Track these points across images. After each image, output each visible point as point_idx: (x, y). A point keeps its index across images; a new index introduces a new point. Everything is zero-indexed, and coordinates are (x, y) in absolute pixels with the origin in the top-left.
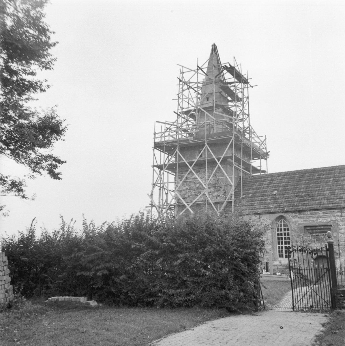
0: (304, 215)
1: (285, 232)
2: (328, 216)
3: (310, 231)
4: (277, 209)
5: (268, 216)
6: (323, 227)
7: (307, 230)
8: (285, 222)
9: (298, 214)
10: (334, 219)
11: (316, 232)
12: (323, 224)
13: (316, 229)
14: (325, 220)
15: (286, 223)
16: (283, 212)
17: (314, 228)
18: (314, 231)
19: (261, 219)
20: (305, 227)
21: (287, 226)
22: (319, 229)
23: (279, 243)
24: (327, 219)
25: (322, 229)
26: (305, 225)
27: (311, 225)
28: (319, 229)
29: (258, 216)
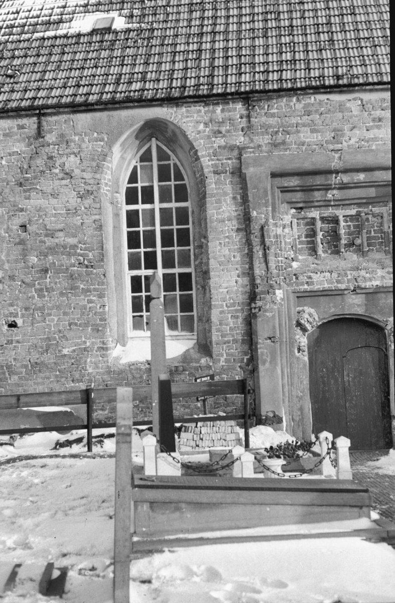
0: (273, 115)
1: (165, 205)
3: (299, 196)
4: (136, 86)
5: (83, 119)
6: (362, 176)
7: (285, 190)
8: (168, 158)
9: (239, 107)
11: (327, 204)
13: (327, 188)
14: (375, 139)
15: (173, 160)
16: (169, 100)
17: (319, 180)
18: (318, 195)
19: (50, 138)
20: (274, 175)
21: (179, 176)
22: (343, 187)
23: (134, 263)
25: (358, 186)
26: (275, 165)
27: (307, 166)
29: (30, 123)
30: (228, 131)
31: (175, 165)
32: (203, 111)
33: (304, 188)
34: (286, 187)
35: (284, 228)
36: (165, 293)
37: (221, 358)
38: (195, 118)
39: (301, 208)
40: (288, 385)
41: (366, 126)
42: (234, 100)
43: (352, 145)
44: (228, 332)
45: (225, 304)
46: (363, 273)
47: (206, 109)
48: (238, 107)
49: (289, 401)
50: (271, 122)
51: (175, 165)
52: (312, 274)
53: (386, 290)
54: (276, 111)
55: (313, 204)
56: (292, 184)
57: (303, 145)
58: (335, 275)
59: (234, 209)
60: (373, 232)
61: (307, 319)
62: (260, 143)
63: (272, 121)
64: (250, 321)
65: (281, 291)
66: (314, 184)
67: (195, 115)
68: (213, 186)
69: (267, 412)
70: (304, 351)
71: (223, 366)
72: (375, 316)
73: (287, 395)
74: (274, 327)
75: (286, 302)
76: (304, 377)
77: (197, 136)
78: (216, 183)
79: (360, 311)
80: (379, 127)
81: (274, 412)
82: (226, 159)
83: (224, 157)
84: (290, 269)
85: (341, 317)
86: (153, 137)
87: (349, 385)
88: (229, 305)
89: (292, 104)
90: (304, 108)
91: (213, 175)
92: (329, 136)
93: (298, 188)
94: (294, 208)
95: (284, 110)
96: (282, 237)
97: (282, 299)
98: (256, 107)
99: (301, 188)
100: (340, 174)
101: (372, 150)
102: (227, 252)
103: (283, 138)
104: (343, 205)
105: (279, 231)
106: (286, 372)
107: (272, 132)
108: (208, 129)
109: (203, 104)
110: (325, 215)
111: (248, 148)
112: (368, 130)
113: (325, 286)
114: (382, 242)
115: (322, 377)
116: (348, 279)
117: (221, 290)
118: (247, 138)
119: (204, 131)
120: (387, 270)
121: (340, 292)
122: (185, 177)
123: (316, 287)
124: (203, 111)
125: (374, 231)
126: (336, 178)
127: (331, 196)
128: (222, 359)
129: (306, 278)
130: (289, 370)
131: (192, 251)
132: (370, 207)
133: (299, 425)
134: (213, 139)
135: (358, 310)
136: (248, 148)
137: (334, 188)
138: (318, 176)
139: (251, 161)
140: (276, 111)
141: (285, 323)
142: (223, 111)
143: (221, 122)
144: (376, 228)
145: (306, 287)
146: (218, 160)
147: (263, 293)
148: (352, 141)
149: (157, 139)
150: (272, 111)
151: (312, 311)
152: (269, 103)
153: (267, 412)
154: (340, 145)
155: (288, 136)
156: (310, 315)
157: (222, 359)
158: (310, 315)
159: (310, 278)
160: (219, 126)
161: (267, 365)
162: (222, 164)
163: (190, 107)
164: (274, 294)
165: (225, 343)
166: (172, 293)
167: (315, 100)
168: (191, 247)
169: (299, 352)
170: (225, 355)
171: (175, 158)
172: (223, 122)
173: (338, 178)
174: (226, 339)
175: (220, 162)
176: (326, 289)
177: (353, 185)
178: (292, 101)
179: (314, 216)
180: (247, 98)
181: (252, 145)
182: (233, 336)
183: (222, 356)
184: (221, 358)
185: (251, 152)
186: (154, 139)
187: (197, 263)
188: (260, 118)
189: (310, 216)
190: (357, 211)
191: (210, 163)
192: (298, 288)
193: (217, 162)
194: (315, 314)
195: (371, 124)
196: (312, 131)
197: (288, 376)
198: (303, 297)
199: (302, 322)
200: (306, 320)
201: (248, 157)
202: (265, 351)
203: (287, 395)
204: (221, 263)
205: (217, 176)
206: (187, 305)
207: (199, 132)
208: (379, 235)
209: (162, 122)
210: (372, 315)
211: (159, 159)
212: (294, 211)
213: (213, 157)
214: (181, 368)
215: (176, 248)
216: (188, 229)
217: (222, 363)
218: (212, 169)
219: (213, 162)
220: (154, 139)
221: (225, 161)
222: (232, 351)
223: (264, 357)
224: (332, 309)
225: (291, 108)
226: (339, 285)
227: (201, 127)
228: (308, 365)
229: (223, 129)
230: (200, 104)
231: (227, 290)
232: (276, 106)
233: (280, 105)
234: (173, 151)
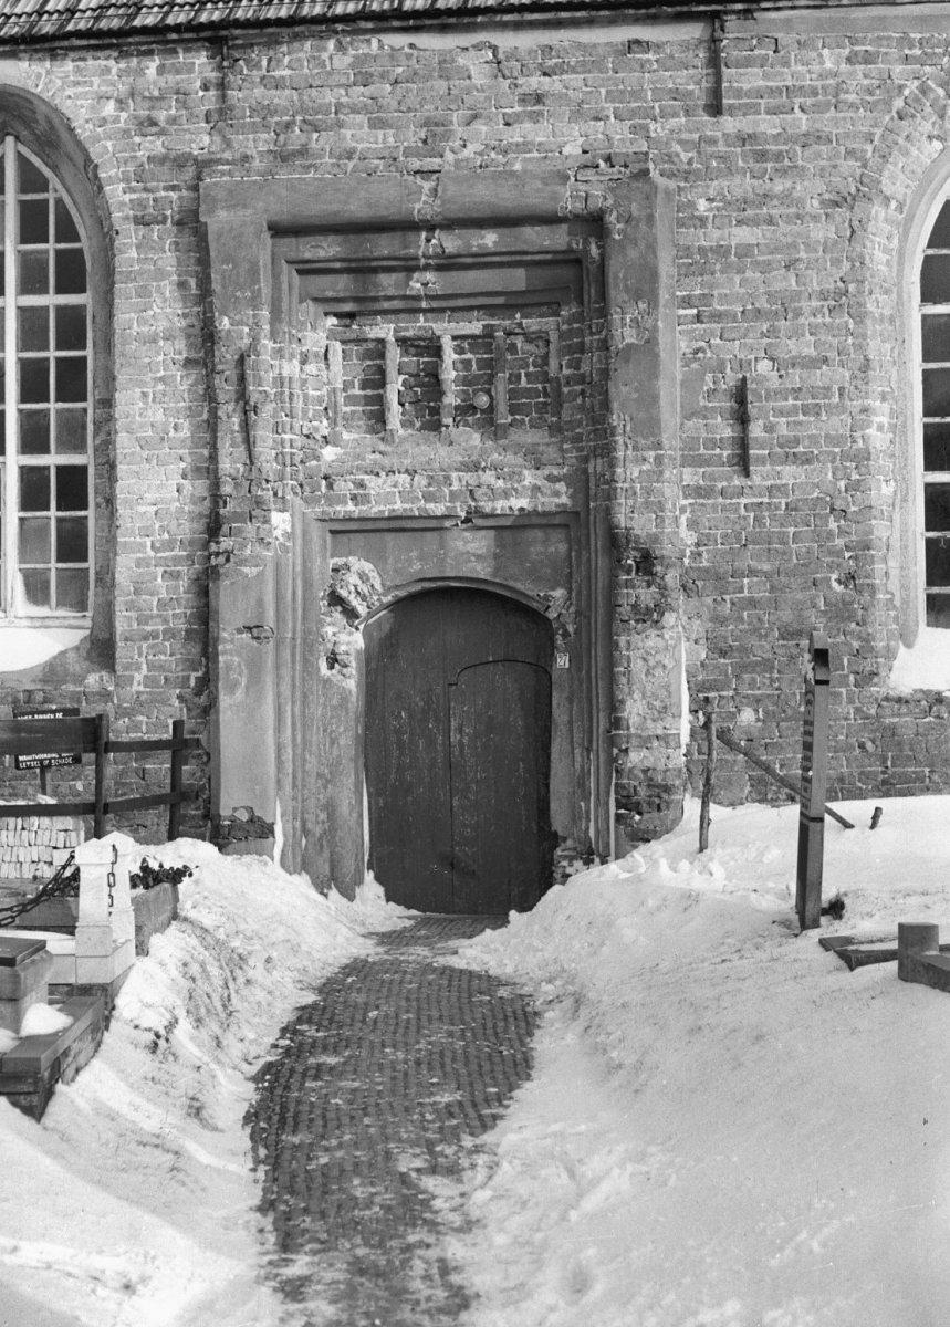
0: (278, 84)
2: (562, 98)
6: (490, 239)
7: (307, 269)
8: (43, 185)
9: (200, 62)
10: (620, 136)
12: (506, 198)
13: (409, 266)
14: (524, 147)
15: (55, 192)
17: (385, 246)
18: (388, 283)
20: (278, 230)
21: (67, 231)
22: (446, 264)
24: (537, 133)
25: (481, 261)
26: (282, 207)
27: (357, 209)
28: (446, 264)
30: (173, 121)
31: (59, 201)
32: (114, 71)
33: (353, 265)
34: (308, 261)
35: (304, 362)
36: (22, 514)
37: (136, 675)
38: (95, 87)
39: (352, 316)
40: (294, 746)
41: (504, 115)
42: (188, 45)
43: (467, 160)
44: (155, 611)
45: (149, 544)
46: (488, 477)
47: (123, 65)
48: (197, 62)
49: (294, 786)
50: (276, 101)
51: (59, 201)
52: (366, 477)
53: (544, 521)
54: (287, 72)
55: (377, 306)
56: (322, 254)
57: (350, 158)
58: (420, 480)
59: (180, 312)
60: (523, 379)
61: (355, 586)
62: (249, 153)
63: (281, 98)
64: (205, 586)
65: (287, 515)
66: (375, 255)
67: (97, 81)
68: (133, 253)
69: (235, 809)
70: (346, 666)
71: (139, 693)
72: (519, 586)
73: (289, 769)
74: (260, 603)
75: (299, 541)
76: (341, 729)
77: (99, 130)
78: (138, 247)
79: (482, 571)
80: (535, 118)
81: (250, 810)
82: (166, 189)
83: (162, 184)
84: (314, 463)
85: (440, 584)
86: (8, 134)
87: (462, 751)
88: (158, 545)
89: (325, 56)
90: (352, 66)
91: (132, 226)
92: (413, 136)
93: (338, 265)
94: (336, 315)
95: (306, 70)
96: (296, 385)
97: (289, 536)
98: (241, 62)
99: (344, 265)
100: (437, 232)
101: (513, 174)
102: (160, 417)
103: (303, 141)
104: (453, 310)
105: (291, 368)
106: (289, 713)
107: (277, 123)
108: (124, 115)
109: (116, 54)
110: (409, 334)
111: (219, 161)
112: (507, 124)
113: (396, 507)
114: (545, 404)
115: (398, 732)
116: (451, 491)
117: (142, 509)
118: (217, 139)
119: (116, 120)
120: (546, 472)
121: (433, 524)
122: (82, 232)
123: (375, 510)
124: (114, 71)
125: (527, 375)
126: (428, 241)
127: (419, 285)
128: (138, 677)
129: (352, 486)
130: (297, 709)
131: (90, 412)
132: (518, 316)
133: (321, 846)
134: (137, 139)
135: (479, 568)
136: (219, 161)
137: (427, 268)
138: (384, 236)
139: (221, 194)
140: (287, 72)
141: (294, 593)
142: (161, 70)
143: (157, 99)
144: (531, 369)
145: (350, 507)
146: (146, 190)
147: (237, 517)
148: (468, 152)
149: (17, 138)
150: (277, 73)
151: (367, 567)
152: (271, 53)
153: (235, 809)
154: (438, 160)
155: (315, 135)
156: (363, 577)
157: (138, 677)
158: (363, 577)
159: (361, 485)
160: (152, 108)
161: (239, 694)
162: (155, 200)
163: (84, 59)
164: (267, 521)
165: (145, 638)
166: (38, 514)
167: (381, 47)
168: (89, 405)
169: (331, 667)
170: (144, 666)
171: (59, 186)
172: (161, 98)
173: (434, 241)
174: (149, 628)
175: (151, 196)
176: (399, 513)
177: (469, 260)
178: (325, 49)
179: (382, 336)
180: (218, 38)
181: (227, 155)
182: (166, 621)
183: (139, 669)
184: (136, 675)
185: (223, 173)
186: (10, 140)
187: (97, 442)
188: (248, 93)
189: (371, 336)
190: (484, 326)
191: (127, 197)
192: (330, 510)
193: (145, 195)
194: (375, 574)
195: (518, 109)
196: (376, 124)
197: (294, 724)
198: (346, 531)
199: (343, 593)
200: (352, 588)
201: (216, 184)
202: (236, 659)
203: (290, 771)
204: (143, 444)
205: (142, 230)
206: (72, 544)
207: (104, 122)
208: (540, 386)
209: (18, 95)
210: (511, 583)
211: (23, 189)
212: (333, 321)
213: (134, 184)
214: (39, 696)
215: (53, 406)
216: (84, 359)
217: (137, 687)
218: (131, 212)
219: (134, 196)
220: (10, 140)
221: (163, 194)
222: (163, 657)
223: (233, 675)
224: (416, 564)
225: (324, 66)
226: (430, 506)
227: (109, 108)
228: (354, 699)
229: (161, 116)
230: (107, 52)
231: (155, 508)
232: (287, 59)
233: (295, 60)
234: (54, 168)
